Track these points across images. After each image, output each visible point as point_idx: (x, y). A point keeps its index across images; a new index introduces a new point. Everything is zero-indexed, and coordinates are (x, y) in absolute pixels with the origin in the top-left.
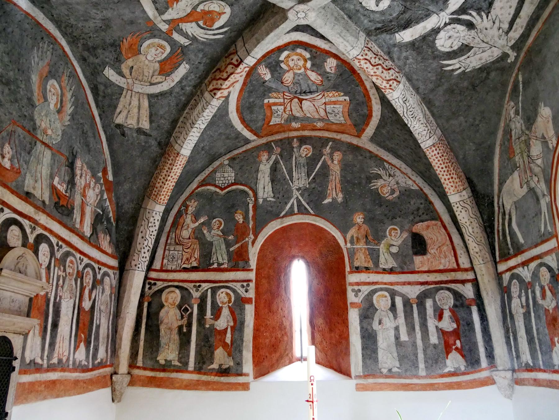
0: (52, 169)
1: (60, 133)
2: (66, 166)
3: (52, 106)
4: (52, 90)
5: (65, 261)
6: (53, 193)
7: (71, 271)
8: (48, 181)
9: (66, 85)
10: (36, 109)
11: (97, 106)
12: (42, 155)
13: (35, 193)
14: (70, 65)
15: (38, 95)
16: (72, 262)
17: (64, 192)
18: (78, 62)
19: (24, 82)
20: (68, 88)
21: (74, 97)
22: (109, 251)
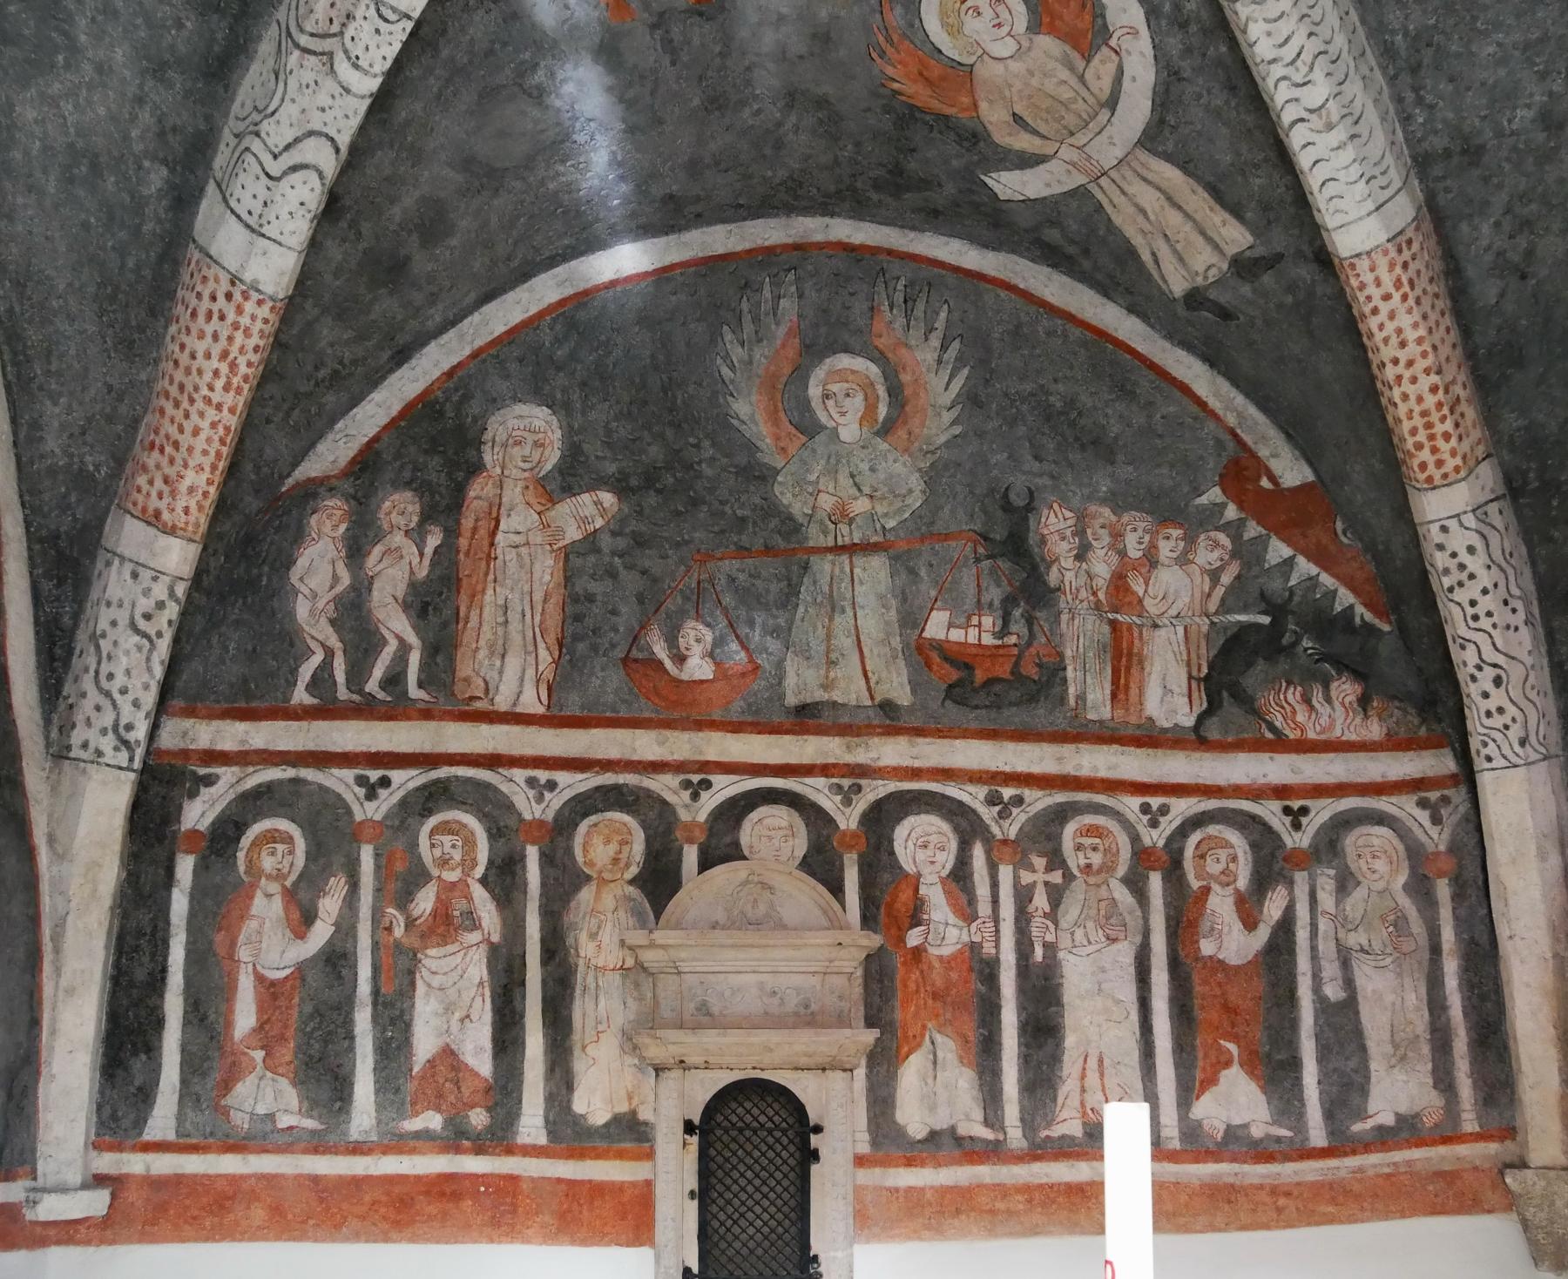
0: (905, 600)
1: (915, 482)
2: (978, 560)
3: (850, 431)
4: (835, 388)
5: (1055, 839)
6: (928, 665)
7: (1096, 859)
8: (896, 642)
9: (899, 332)
10: (780, 478)
11: (1106, 289)
12: (845, 584)
13: (837, 696)
14: (895, 268)
15: (777, 438)
16: (1092, 831)
17: (987, 640)
18: (938, 231)
19: (706, 443)
20: (915, 336)
21: (956, 345)
22: (1375, 730)
